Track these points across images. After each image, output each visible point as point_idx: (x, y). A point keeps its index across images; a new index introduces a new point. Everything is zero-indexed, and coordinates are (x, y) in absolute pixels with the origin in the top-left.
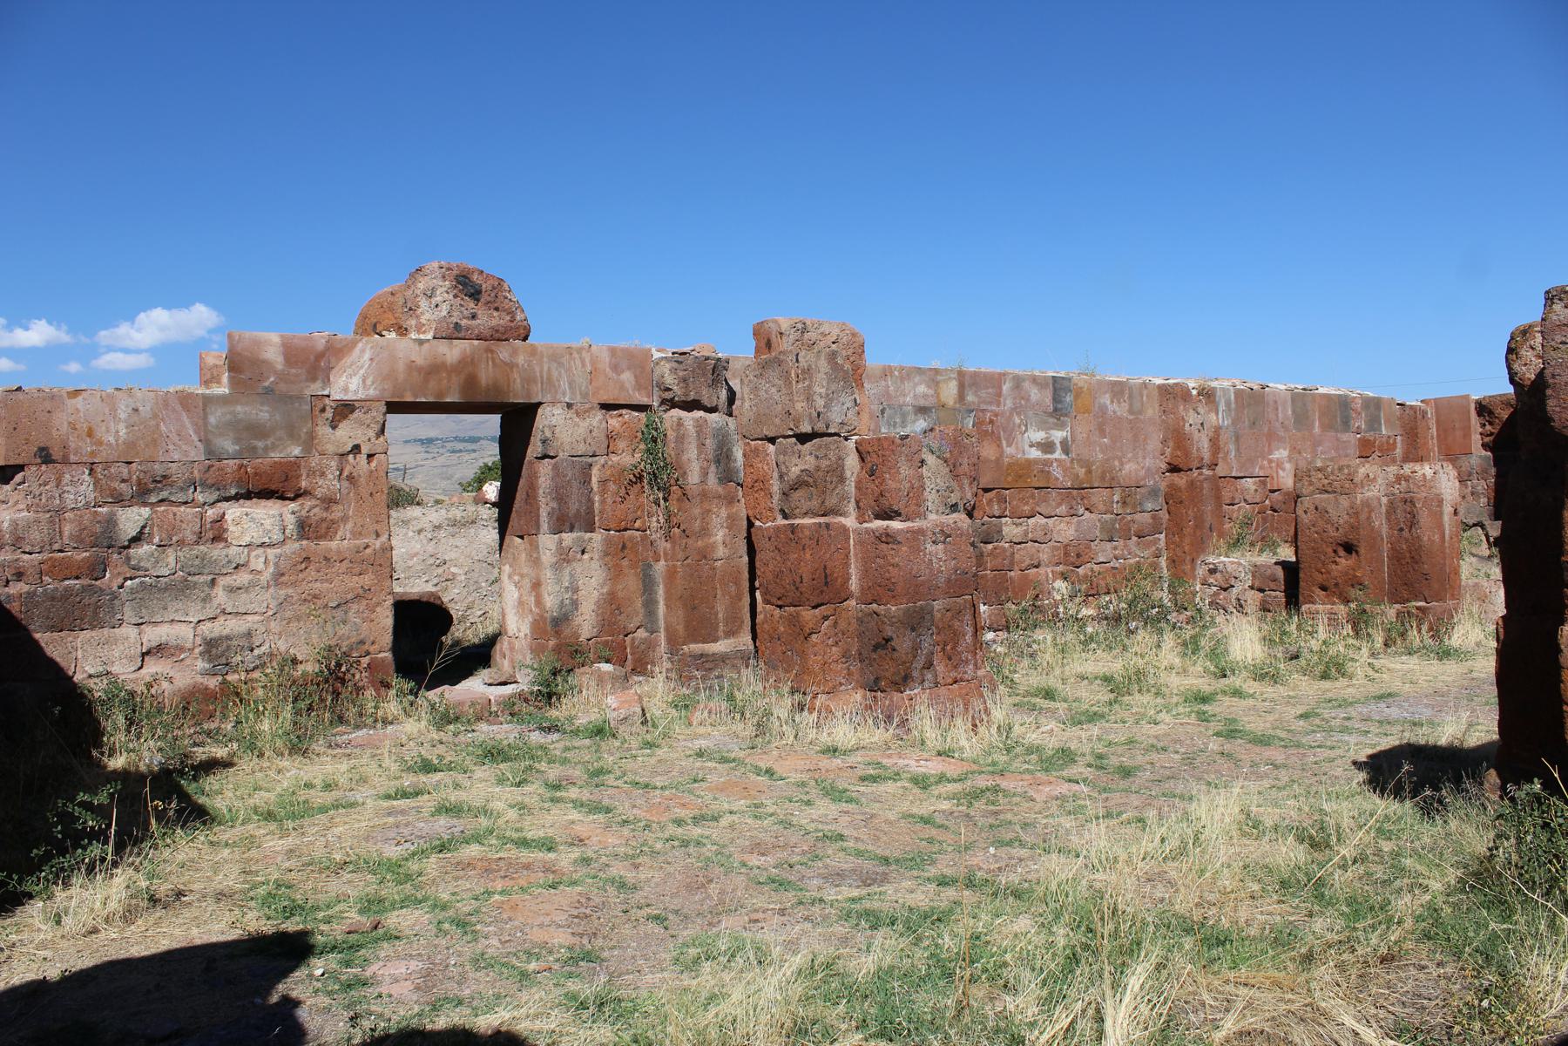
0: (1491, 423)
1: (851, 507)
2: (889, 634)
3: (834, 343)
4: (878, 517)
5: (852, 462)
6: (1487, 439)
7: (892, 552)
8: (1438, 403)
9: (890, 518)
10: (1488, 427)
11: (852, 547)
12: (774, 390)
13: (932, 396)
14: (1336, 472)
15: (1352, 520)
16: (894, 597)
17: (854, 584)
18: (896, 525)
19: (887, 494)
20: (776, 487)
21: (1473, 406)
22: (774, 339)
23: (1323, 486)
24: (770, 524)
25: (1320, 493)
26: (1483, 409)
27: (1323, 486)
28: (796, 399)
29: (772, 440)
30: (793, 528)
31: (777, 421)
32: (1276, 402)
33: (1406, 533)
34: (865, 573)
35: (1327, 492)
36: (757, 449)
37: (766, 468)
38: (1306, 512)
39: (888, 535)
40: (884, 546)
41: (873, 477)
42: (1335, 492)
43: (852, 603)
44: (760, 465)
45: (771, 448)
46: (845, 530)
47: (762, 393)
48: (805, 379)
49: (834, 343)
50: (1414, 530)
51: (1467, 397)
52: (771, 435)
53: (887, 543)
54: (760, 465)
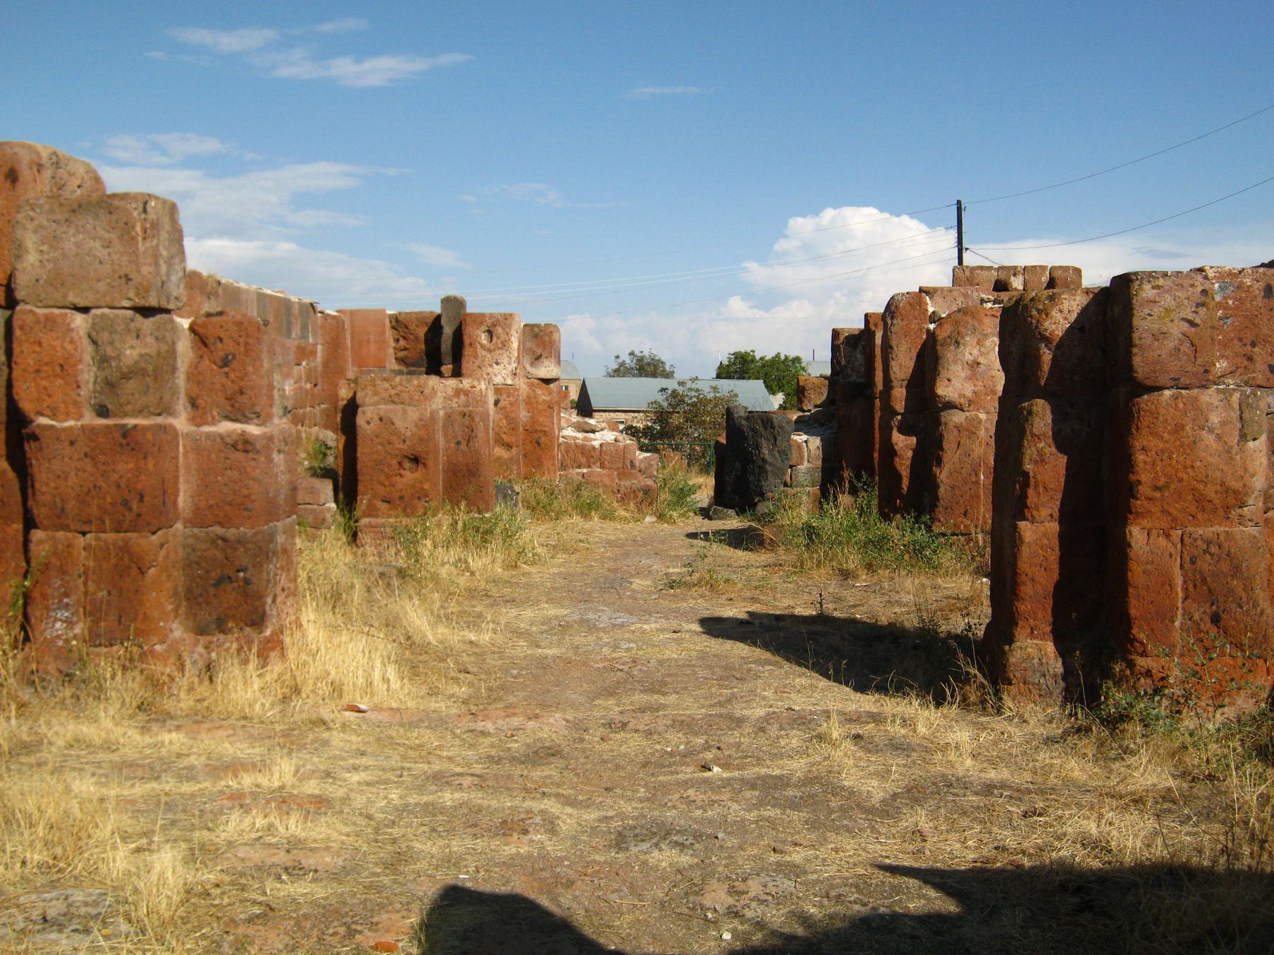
0: (404, 338)
1: (181, 405)
2: (244, 564)
3: (79, 187)
4: (227, 418)
5: (184, 346)
6: (402, 354)
7: (252, 463)
8: (353, 313)
9: (246, 420)
10: (402, 343)
11: (181, 455)
12: (97, 244)
13: (144, 264)
14: (404, 383)
15: (421, 433)
16: (250, 518)
17: (183, 500)
18: (253, 430)
19: (249, 392)
20: (88, 375)
21: (388, 323)
22: (25, 173)
23: (390, 396)
24: (71, 423)
25: (385, 404)
26: (399, 323)
27: (390, 396)
28: (141, 260)
29: (85, 310)
30: (126, 432)
31: (101, 287)
32: (247, 301)
33: (463, 446)
34: (205, 484)
35: (393, 402)
36: (48, 318)
37: (69, 347)
38: (368, 423)
39: (246, 442)
40: (240, 456)
41: (226, 369)
42: (403, 403)
43: (179, 526)
44: (57, 343)
45: (79, 320)
46: (174, 433)
47: (69, 245)
48: (154, 236)
49: (79, 187)
50: (471, 442)
51: (382, 312)
52: (82, 304)
53: (246, 451)
54: (57, 343)
